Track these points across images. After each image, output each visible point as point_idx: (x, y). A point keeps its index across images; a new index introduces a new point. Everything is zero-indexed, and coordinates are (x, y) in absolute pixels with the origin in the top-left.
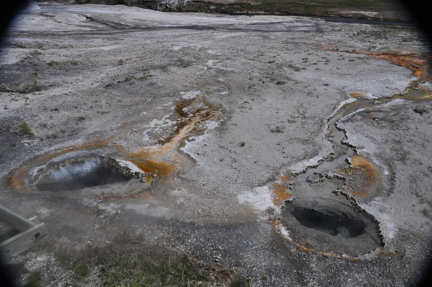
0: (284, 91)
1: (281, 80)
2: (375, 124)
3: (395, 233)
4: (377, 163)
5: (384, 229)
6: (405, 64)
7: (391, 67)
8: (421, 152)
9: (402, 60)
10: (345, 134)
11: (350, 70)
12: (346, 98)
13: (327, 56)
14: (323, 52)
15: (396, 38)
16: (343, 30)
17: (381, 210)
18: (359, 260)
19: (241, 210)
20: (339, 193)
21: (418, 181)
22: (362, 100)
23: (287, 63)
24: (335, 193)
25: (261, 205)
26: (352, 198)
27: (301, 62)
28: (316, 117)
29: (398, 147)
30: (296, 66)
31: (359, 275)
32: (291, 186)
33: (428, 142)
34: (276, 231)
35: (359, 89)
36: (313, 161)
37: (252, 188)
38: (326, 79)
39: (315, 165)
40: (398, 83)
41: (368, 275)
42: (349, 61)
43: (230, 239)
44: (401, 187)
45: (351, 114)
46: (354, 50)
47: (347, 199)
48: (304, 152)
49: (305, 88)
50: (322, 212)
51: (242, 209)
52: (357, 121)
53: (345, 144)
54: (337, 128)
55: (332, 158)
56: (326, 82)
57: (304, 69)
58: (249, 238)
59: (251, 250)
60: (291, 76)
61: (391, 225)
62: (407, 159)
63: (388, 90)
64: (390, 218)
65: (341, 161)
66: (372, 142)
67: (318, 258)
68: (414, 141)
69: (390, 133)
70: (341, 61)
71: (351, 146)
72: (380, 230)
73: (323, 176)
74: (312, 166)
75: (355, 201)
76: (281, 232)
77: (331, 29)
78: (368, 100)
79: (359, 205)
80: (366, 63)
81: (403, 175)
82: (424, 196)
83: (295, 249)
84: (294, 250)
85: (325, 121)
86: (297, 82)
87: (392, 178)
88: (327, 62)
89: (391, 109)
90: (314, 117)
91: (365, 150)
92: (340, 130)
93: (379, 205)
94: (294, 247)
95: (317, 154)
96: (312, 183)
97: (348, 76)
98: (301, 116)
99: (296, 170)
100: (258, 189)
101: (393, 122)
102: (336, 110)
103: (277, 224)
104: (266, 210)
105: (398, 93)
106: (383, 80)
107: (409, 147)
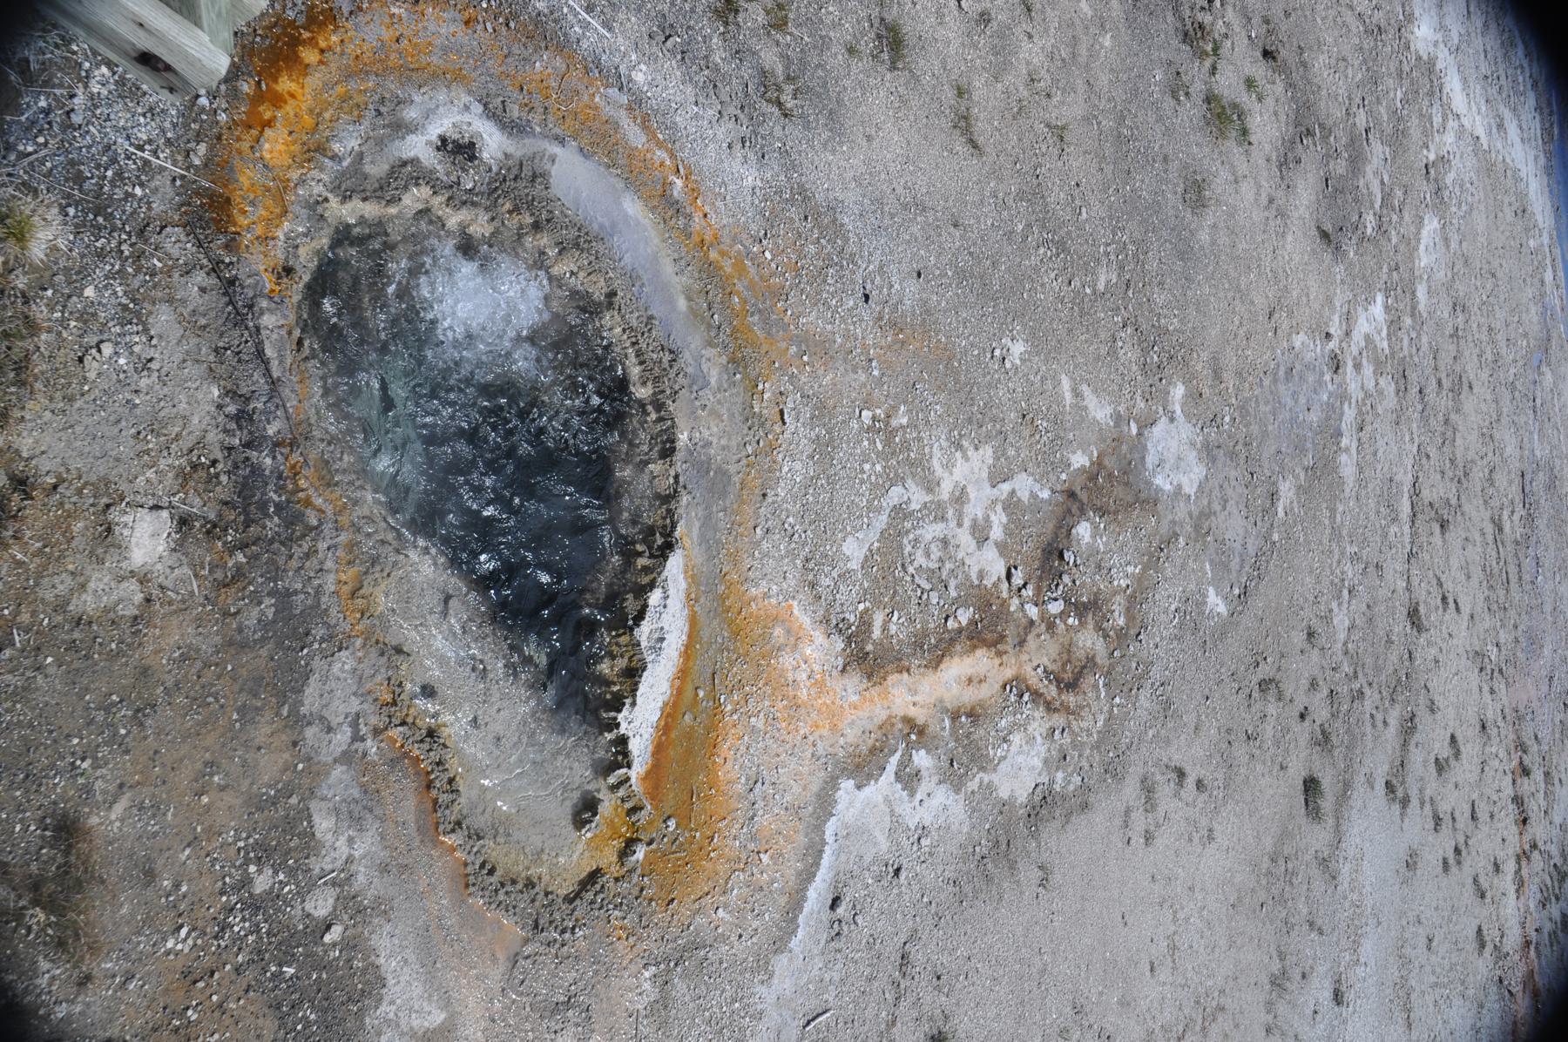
1: (1327, 782)
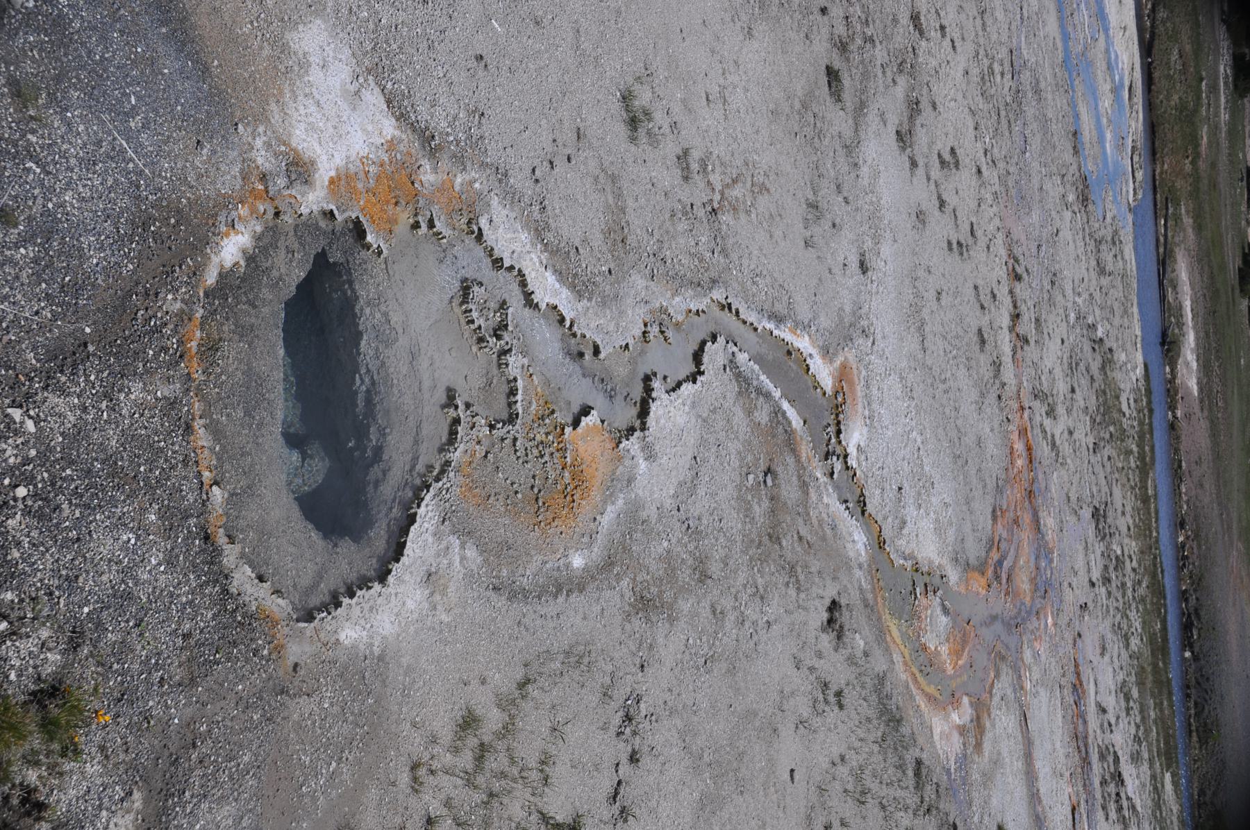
0: (805, 106)
1: (846, 82)
2: (751, 477)
3: (362, 647)
4: (607, 519)
5: (366, 607)
6: (1005, 535)
7: (985, 487)
8: (687, 657)
9: (1016, 521)
10: (687, 380)
11: (940, 342)
12: (826, 353)
13: (982, 241)
14: (997, 222)
15: (1104, 482)
16: (1105, 281)
17: (433, 578)
18: (217, 552)
19: (261, 48)
20: (452, 413)
21: (577, 672)
22: (832, 413)
23: (925, 91)
24: (450, 399)
25: (311, 128)
26: (448, 463)
27: (939, 146)
28: (727, 256)
29: (684, 575)
30: (918, 128)
31: (160, 564)
32: (424, 226)
33: (728, 671)
34: (224, 213)
35: (875, 391)
36: (548, 288)
37: (369, 71)
38: (888, 259)
39: (536, 298)
40: (927, 525)
41: (171, 595)
42: (980, 331)
43: (122, 32)
44: (538, 622)
45: (768, 384)
46: (1027, 341)
47: (441, 450)
48: (577, 243)
49: (833, 187)
50: (363, 371)
51: (266, 51)
52: (749, 413)
53: (648, 390)
54: (703, 343)
55: (581, 355)
56: (872, 261)
57: (914, 164)
58: (155, 110)
59: (109, 133)
60: (872, 117)
61: (387, 625)
62: (648, 620)
63: (891, 494)
64: (415, 616)
65: (579, 391)
66: (680, 484)
67: (173, 403)
68: (722, 627)
69: (729, 540)
70: (973, 299)
71: (644, 413)
72: (359, 593)
73: (499, 338)
74: (530, 288)
75: (437, 479)
76: (227, 235)
77: (1103, 232)
78: (839, 432)
79: (428, 498)
80: (982, 395)
81: (585, 618)
82: (527, 706)
83: (178, 305)
84: (172, 303)
85: (718, 294)
86: (850, 149)
87: (564, 586)
88: (959, 248)
89: (820, 522)
90: (723, 251)
91: (643, 465)
92: (698, 357)
93: (450, 564)
94: (183, 301)
95: (580, 296)
96: (462, 304)
97: (917, 339)
98: (717, 197)
99: (496, 229)
100: (373, 98)
101: (775, 538)
102: (770, 326)
103: (253, 211)
104: (295, 150)
105: (887, 533)
106: (927, 468)
107: (694, 615)
